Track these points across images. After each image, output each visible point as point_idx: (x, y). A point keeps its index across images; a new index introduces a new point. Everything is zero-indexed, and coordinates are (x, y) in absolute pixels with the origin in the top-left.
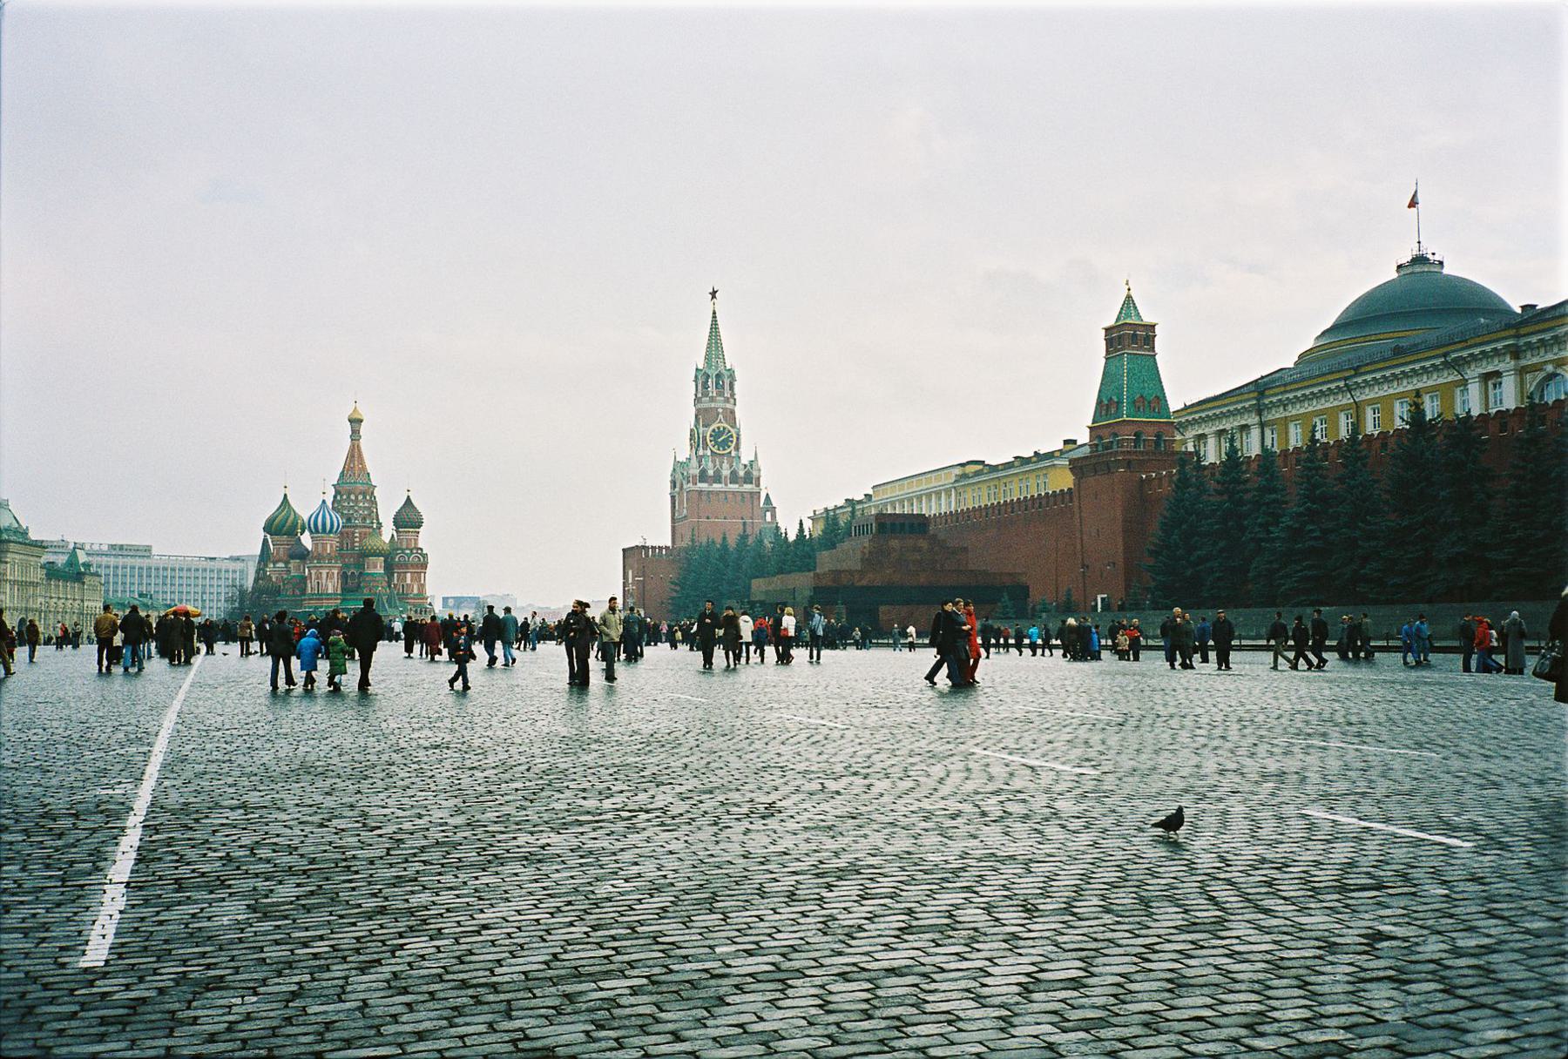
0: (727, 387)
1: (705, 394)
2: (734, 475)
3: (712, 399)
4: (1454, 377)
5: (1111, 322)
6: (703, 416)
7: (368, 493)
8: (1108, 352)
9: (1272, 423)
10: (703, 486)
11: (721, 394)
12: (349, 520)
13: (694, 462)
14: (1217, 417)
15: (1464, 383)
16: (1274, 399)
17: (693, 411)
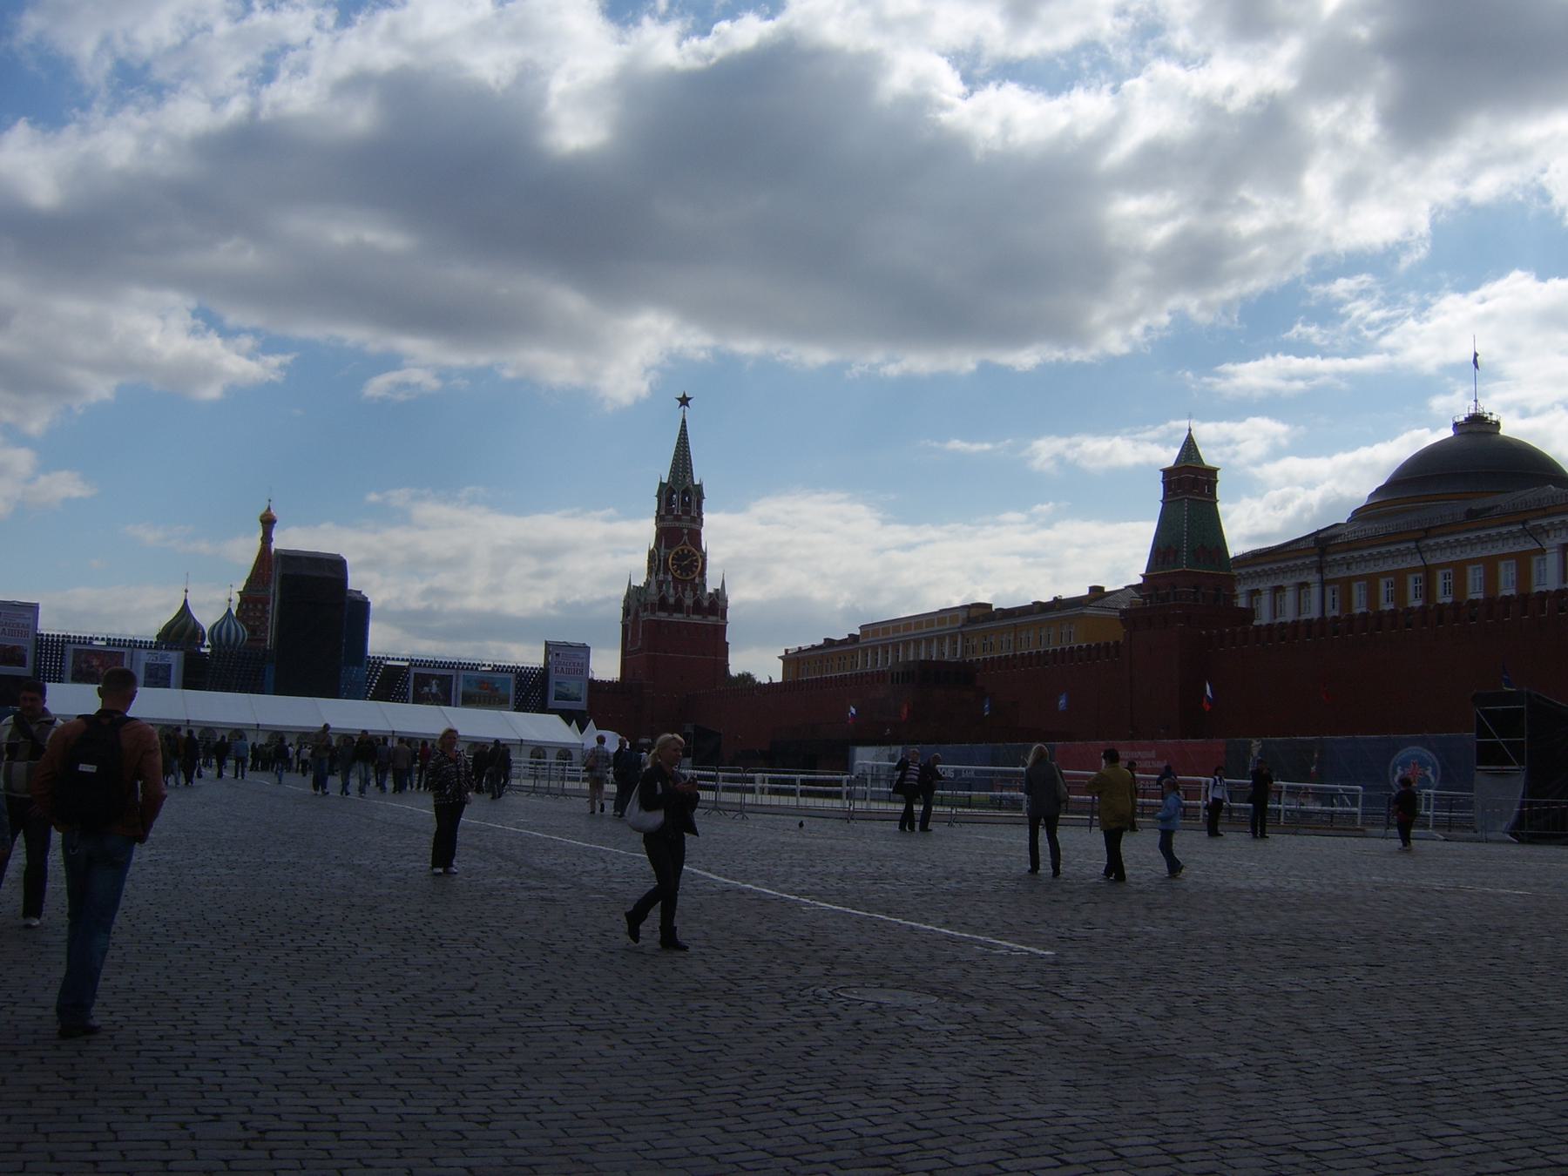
0: (694, 505)
1: (669, 511)
2: (698, 603)
3: (678, 518)
4: (1531, 545)
9: (1334, 581)
10: (663, 616)
11: (687, 513)
14: (1275, 573)
15: (1542, 551)
16: (1338, 557)
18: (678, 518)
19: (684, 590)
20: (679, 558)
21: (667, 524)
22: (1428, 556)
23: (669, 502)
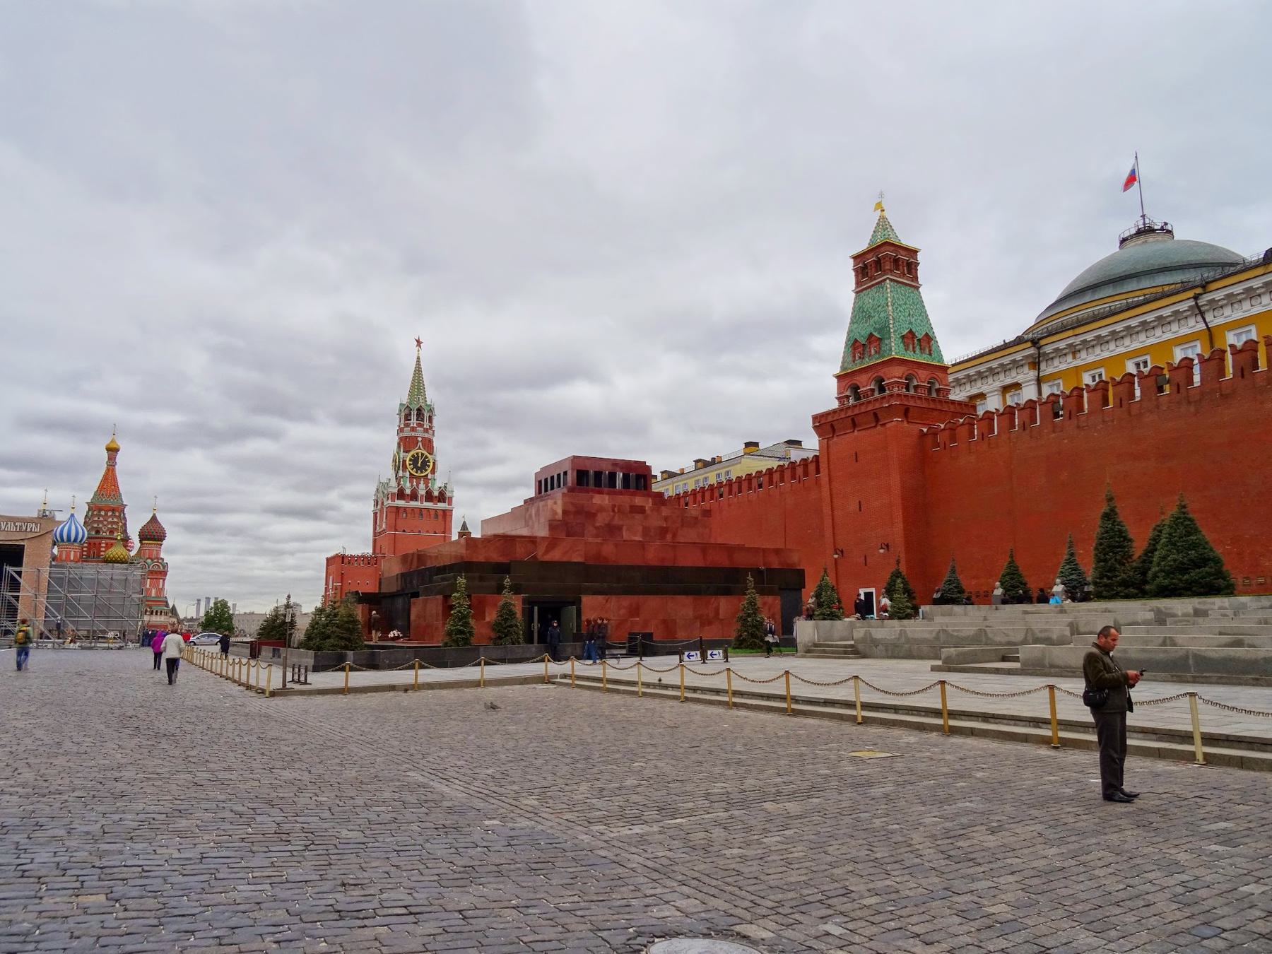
0: (426, 418)
1: (407, 425)
3: (413, 429)
5: (863, 246)
6: (406, 443)
7: (119, 510)
8: (858, 283)
10: (401, 503)
12: (97, 532)
13: (393, 483)
17: (396, 439)
18: (413, 429)
19: (418, 484)
20: (415, 460)
21: (405, 434)
22: (1209, 317)
23: (408, 417)
